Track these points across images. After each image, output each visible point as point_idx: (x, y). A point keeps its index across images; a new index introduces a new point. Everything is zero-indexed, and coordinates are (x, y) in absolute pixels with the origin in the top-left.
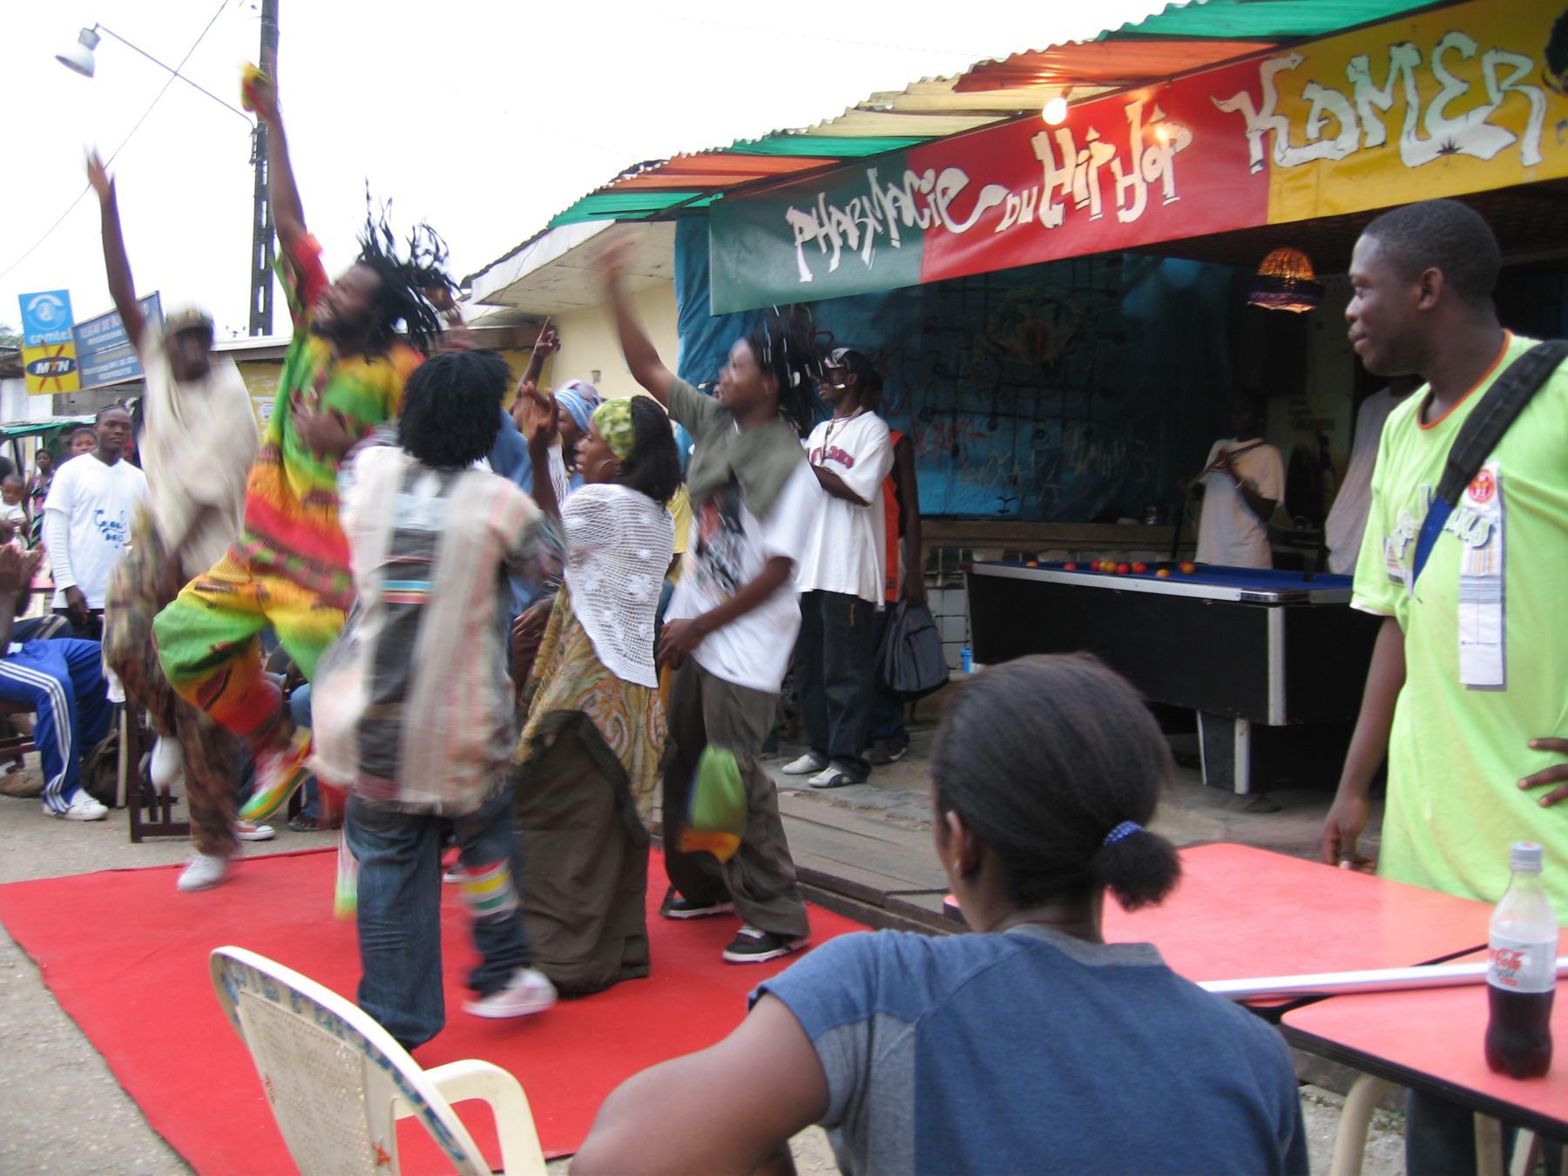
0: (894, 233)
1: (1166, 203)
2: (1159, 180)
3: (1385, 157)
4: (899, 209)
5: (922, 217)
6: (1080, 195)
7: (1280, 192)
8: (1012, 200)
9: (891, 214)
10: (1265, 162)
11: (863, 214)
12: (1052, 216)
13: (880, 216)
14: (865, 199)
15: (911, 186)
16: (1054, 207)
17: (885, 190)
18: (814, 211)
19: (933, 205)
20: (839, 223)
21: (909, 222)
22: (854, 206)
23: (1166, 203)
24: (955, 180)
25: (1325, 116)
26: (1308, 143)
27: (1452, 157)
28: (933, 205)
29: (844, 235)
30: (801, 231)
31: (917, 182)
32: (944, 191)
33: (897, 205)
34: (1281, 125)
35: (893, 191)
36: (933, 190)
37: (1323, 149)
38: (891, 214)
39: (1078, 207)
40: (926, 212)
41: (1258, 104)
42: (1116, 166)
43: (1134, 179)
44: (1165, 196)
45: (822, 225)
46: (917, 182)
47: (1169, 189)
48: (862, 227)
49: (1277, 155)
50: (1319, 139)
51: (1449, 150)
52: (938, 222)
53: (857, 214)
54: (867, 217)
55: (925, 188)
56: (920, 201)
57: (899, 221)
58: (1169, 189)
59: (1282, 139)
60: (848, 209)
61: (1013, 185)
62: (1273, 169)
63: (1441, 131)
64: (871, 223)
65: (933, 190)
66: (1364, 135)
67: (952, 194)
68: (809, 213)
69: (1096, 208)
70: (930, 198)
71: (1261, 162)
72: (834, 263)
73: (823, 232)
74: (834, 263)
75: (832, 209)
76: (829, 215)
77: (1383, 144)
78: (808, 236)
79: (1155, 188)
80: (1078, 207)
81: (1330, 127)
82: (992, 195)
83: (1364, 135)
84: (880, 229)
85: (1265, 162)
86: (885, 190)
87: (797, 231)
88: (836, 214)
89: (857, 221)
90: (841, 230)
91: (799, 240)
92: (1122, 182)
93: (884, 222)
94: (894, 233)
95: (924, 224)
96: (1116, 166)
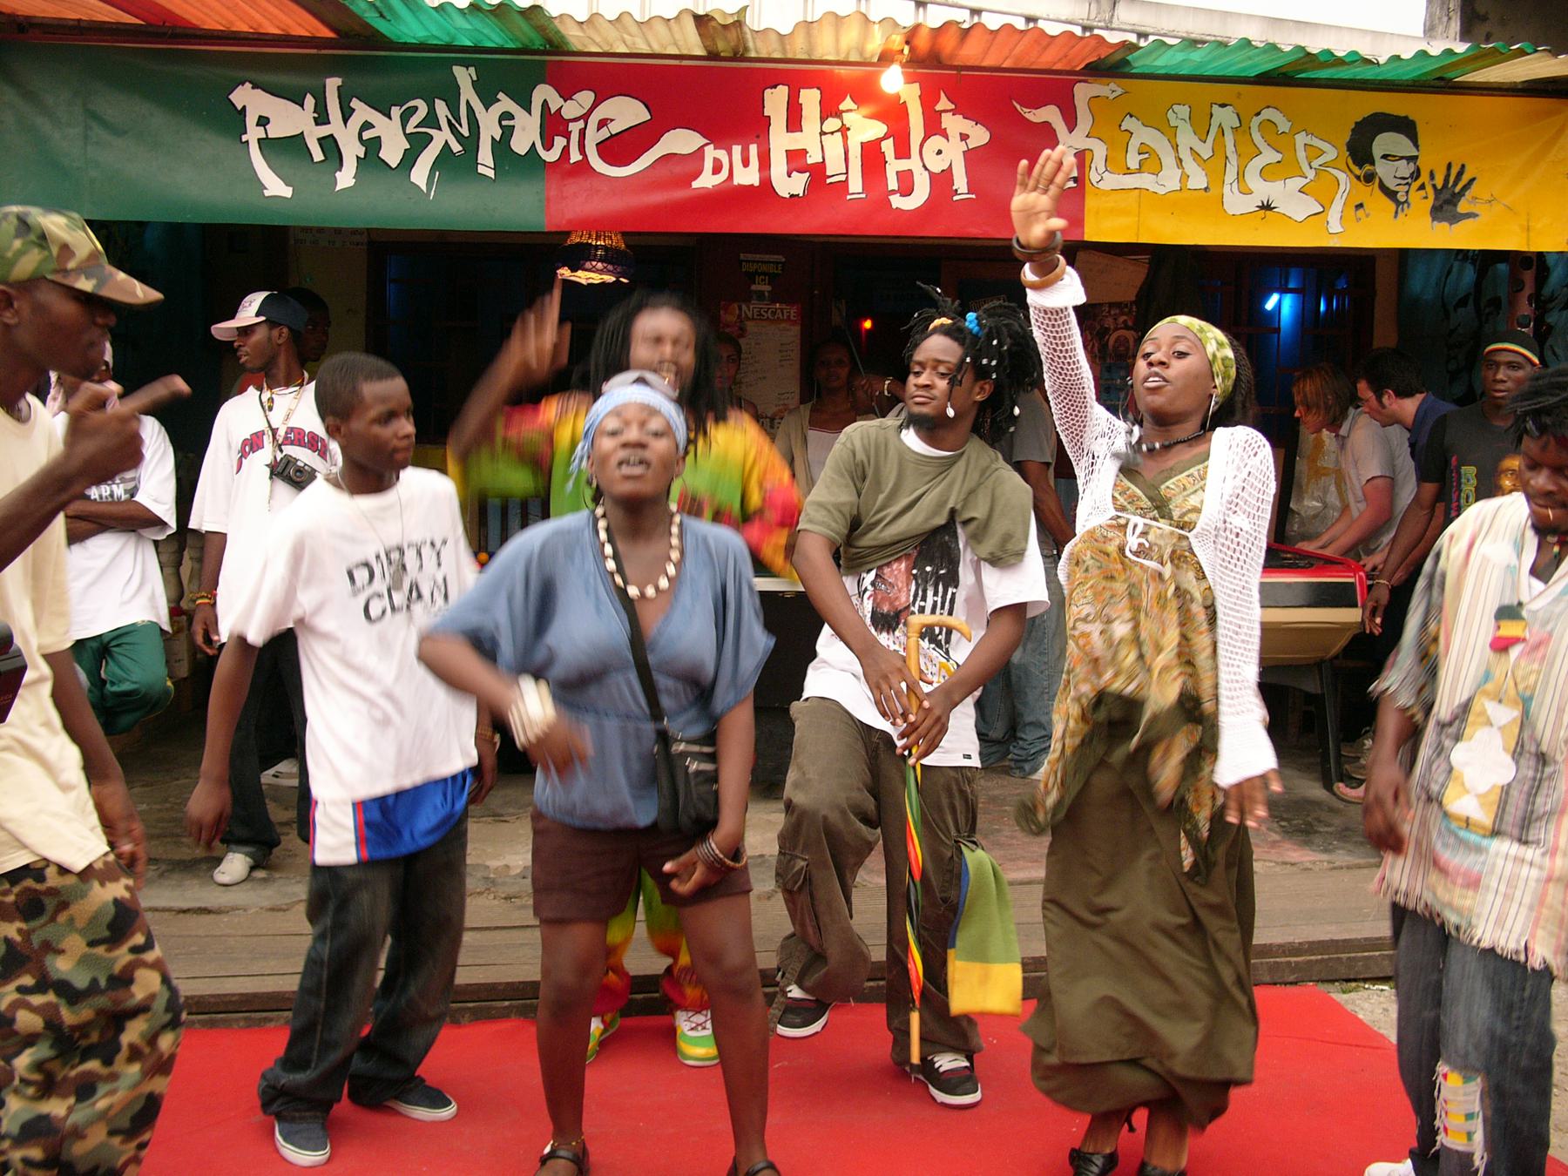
0: (485, 156)
1: (955, 198)
2: (948, 174)
4: (508, 132)
5: (548, 146)
6: (834, 167)
7: (1097, 213)
8: (711, 153)
9: (490, 128)
11: (431, 120)
12: (789, 185)
13: (465, 131)
14: (441, 109)
15: (545, 104)
16: (795, 174)
17: (488, 102)
18: (310, 101)
19: (575, 138)
20: (367, 126)
21: (520, 145)
22: (416, 108)
23: (955, 198)
24: (627, 112)
25: (1144, 150)
26: (1128, 171)
27: (1268, 212)
28: (575, 138)
29: (373, 146)
30: (263, 122)
31: (555, 102)
32: (603, 123)
33: (504, 123)
34: (1099, 150)
35: (505, 103)
36: (585, 117)
37: (1145, 181)
38: (490, 128)
39: (829, 181)
40: (560, 142)
41: (1071, 124)
42: (888, 147)
43: (913, 164)
44: (956, 190)
45: (322, 118)
46: (555, 102)
47: (961, 183)
48: (418, 143)
49: (1093, 176)
50: (1139, 171)
51: (1266, 207)
52: (575, 157)
53: (415, 120)
54: (440, 129)
55: (570, 110)
56: (553, 125)
57: (502, 147)
58: (961, 183)
59: (1098, 162)
60: (396, 112)
61: (719, 133)
63: (1263, 190)
64: (442, 137)
65: (585, 117)
66: (1185, 177)
67: (615, 128)
68: (302, 106)
69: (856, 185)
70: (574, 128)
71: (1075, 180)
72: (346, 178)
73: (324, 131)
74: (346, 178)
75: (355, 103)
76: (347, 114)
77: (1206, 189)
78: (275, 131)
79: (942, 181)
80: (829, 181)
81: (1151, 165)
82: (681, 141)
83: (1185, 177)
84: (456, 147)
86: (488, 102)
87: (251, 120)
88: (362, 112)
89: (409, 129)
90: (367, 135)
91: (253, 134)
92: (894, 166)
93: (471, 143)
94: (485, 156)
95: (552, 156)
96: (888, 147)
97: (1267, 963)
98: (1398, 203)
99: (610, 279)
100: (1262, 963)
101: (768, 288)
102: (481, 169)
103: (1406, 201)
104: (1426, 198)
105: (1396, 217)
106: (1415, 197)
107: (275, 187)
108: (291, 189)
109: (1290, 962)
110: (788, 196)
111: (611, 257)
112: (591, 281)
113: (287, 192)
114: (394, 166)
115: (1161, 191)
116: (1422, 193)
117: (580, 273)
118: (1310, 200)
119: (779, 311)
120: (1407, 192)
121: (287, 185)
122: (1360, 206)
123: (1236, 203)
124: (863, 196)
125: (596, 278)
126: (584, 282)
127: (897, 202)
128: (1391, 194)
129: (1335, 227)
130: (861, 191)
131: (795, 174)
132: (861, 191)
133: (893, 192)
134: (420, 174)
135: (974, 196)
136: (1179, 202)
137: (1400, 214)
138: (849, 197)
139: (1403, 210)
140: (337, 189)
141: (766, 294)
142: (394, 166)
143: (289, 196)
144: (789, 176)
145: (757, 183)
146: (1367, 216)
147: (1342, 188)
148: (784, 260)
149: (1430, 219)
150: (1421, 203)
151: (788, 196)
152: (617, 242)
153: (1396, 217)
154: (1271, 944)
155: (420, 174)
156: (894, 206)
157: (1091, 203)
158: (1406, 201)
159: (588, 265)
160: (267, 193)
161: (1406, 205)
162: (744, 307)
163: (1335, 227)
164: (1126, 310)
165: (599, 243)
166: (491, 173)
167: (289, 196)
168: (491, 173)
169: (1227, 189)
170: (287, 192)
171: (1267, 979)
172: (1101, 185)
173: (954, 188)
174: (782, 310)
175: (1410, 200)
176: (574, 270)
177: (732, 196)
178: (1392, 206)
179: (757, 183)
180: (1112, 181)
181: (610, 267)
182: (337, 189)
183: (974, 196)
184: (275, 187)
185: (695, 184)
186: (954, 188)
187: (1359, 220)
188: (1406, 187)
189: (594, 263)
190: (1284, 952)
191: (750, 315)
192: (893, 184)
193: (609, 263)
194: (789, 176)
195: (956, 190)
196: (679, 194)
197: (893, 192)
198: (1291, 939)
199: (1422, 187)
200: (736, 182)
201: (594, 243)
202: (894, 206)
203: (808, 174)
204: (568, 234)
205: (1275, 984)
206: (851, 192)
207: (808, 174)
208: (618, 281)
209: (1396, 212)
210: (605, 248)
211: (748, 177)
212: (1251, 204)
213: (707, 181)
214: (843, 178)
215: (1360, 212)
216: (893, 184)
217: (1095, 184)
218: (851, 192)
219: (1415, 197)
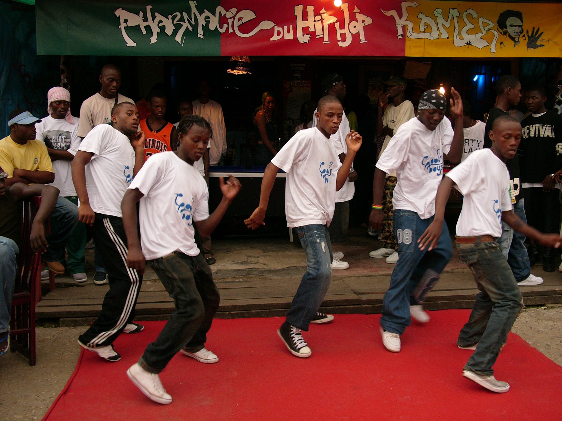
1: (361, 42)
3: (449, 42)
7: (410, 47)
10: (403, 35)
12: (303, 39)
16: (305, 35)
23: (361, 42)
27: (470, 46)
37: (426, 35)
39: (317, 37)
44: (361, 40)
47: (362, 37)
51: (469, 44)
58: (362, 37)
62: (407, 38)
63: (467, 38)
69: (326, 39)
71: (402, 35)
72: (154, 40)
74: (154, 40)
77: (448, 38)
79: (356, 37)
80: (317, 37)
85: (403, 35)
97: (465, 301)
98: (515, 42)
99: (245, 73)
100: (463, 301)
101: (300, 75)
102: (199, 36)
103: (518, 41)
104: (525, 40)
105: (514, 46)
106: (521, 39)
107: (130, 43)
108: (136, 43)
109: (473, 301)
110: (303, 43)
111: (245, 66)
112: (239, 73)
113: (134, 45)
114: (170, 35)
115: (432, 39)
116: (524, 38)
117: (235, 71)
118: (484, 41)
119: (304, 83)
120: (519, 38)
121: (134, 42)
122: (502, 43)
123: (458, 42)
124: (329, 42)
125: (240, 73)
126: (236, 74)
127: (341, 44)
128: (513, 39)
129: (493, 50)
130: (328, 41)
131: (305, 35)
132: (328, 41)
133: (339, 41)
134: (178, 38)
135: (367, 42)
136: (438, 42)
137: (516, 46)
138: (324, 43)
139: (517, 44)
140: (151, 43)
141: (299, 77)
142: (170, 35)
143: (135, 46)
144: (303, 36)
145: (292, 38)
146: (504, 46)
147: (495, 37)
148: (305, 66)
149: (527, 47)
150: (523, 42)
151: (303, 43)
152: (247, 60)
153: (514, 46)
154: (466, 295)
155: (178, 38)
156: (340, 46)
157: (408, 43)
158: (518, 41)
159: (237, 68)
160: (128, 45)
161: (518, 42)
162: (292, 82)
163: (493, 50)
164: (423, 81)
165: (241, 60)
166: (202, 37)
167: (135, 46)
168: (202, 37)
169: (455, 38)
170: (134, 45)
171: (465, 307)
172: (410, 37)
173: (360, 39)
174: (305, 83)
175: (519, 41)
176: (232, 70)
177: (283, 43)
178: (513, 43)
179: (292, 38)
180: (415, 36)
181: (245, 69)
182: (151, 43)
183: (367, 42)
184: (130, 43)
185: (271, 39)
186: (360, 39)
187: (501, 48)
188: (518, 36)
189: (239, 67)
190: (471, 298)
191: (294, 85)
192: (339, 38)
193: (244, 67)
194: (303, 36)
195: (361, 40)
196: (266, 43)
197: (339, 41)
198: (473, 294)
199: (524, 36)
200: (285, 39)
201: (239, 60)
202: (340, 46)
203: (310, 35)
204: (230, 57)
205: (468, 309)
206: (324, 41)
207: (310, 35)
208: (247, 73)
209: (515, 45)
210: (243, 62)
211: (289, 36)
212: (463, 43)
213: (275, 38)
214: (322, 36)
215: (502, 45)
216: (339, 38)
217: (409, 37)
218: (324, 41)
219: (521, 39)
